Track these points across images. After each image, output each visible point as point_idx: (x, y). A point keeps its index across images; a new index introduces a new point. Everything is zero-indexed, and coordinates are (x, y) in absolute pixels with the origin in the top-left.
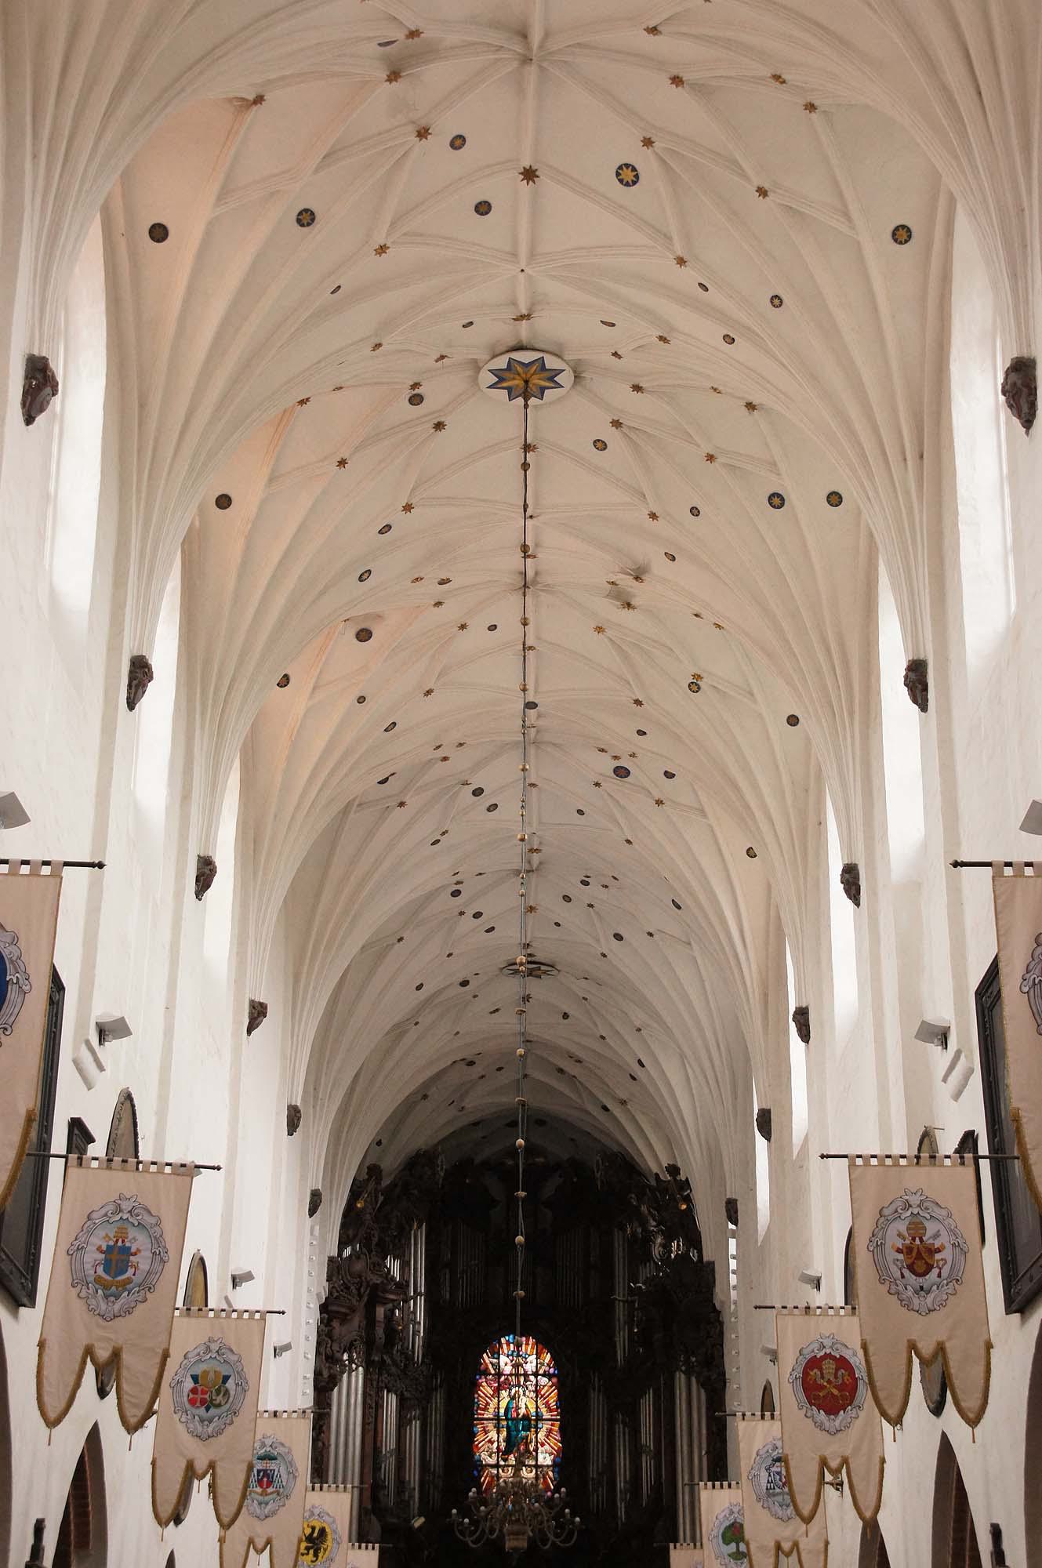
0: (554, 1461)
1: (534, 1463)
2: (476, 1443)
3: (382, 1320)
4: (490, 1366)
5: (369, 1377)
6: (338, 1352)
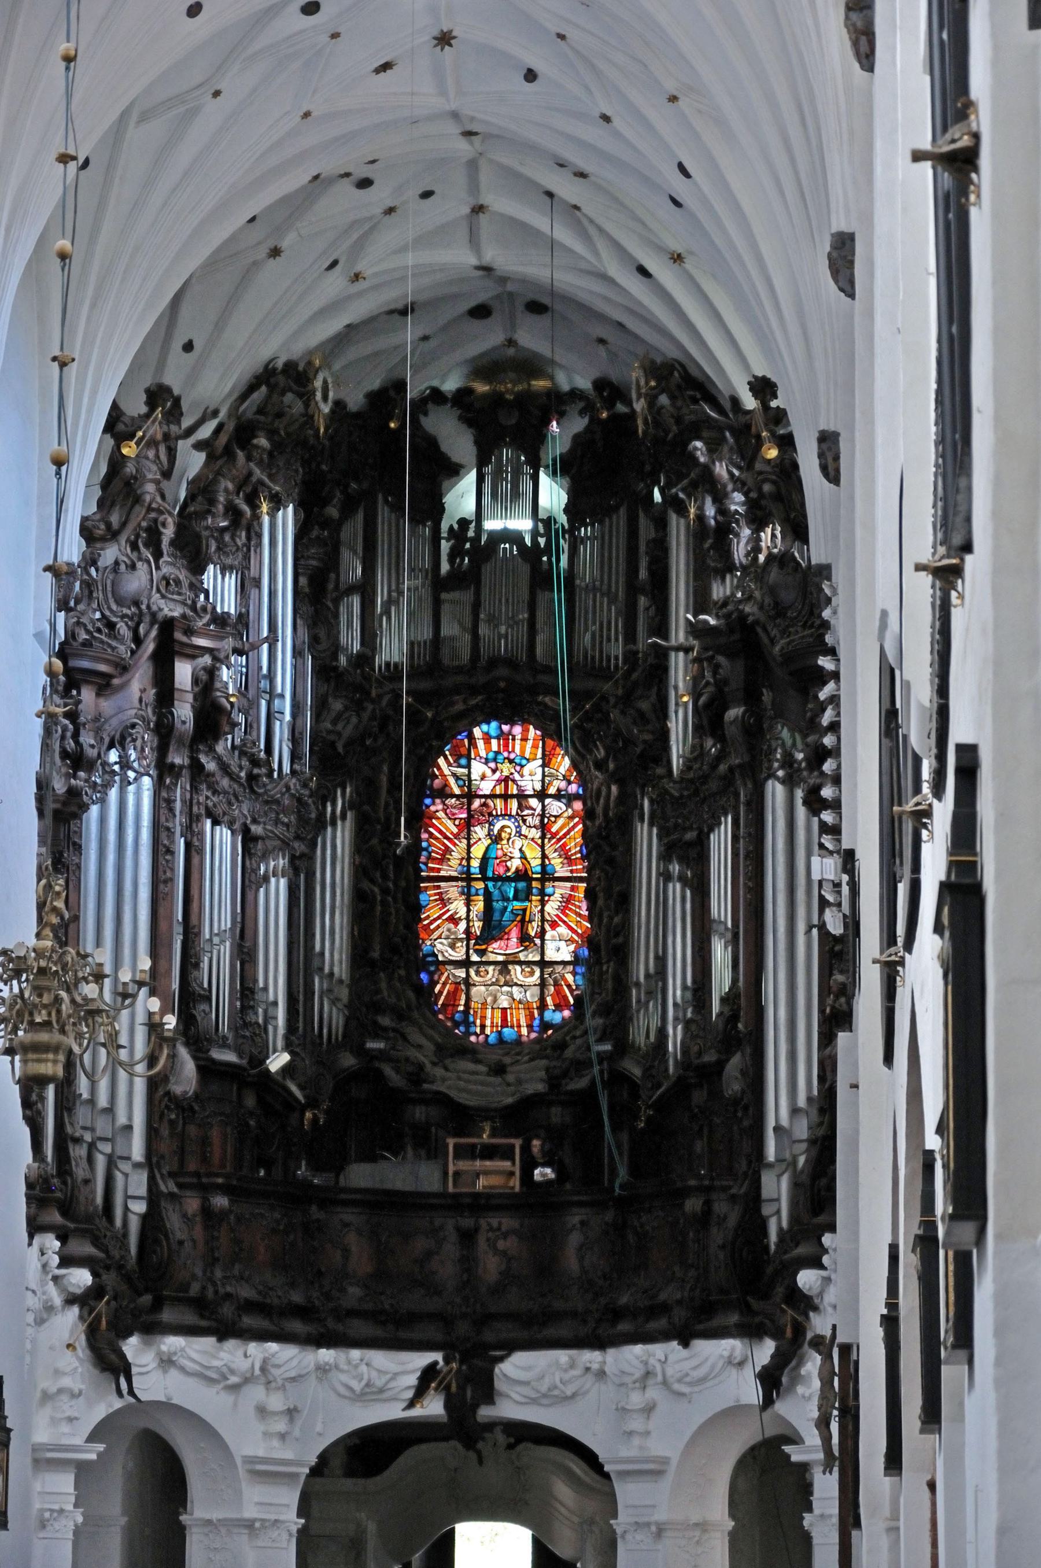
0: (575, 953)
1: (537, 958)
2: (426, 922)
3: (189, 688)
4: (452, 781)
5: (164, 794)
6: (93, 746)
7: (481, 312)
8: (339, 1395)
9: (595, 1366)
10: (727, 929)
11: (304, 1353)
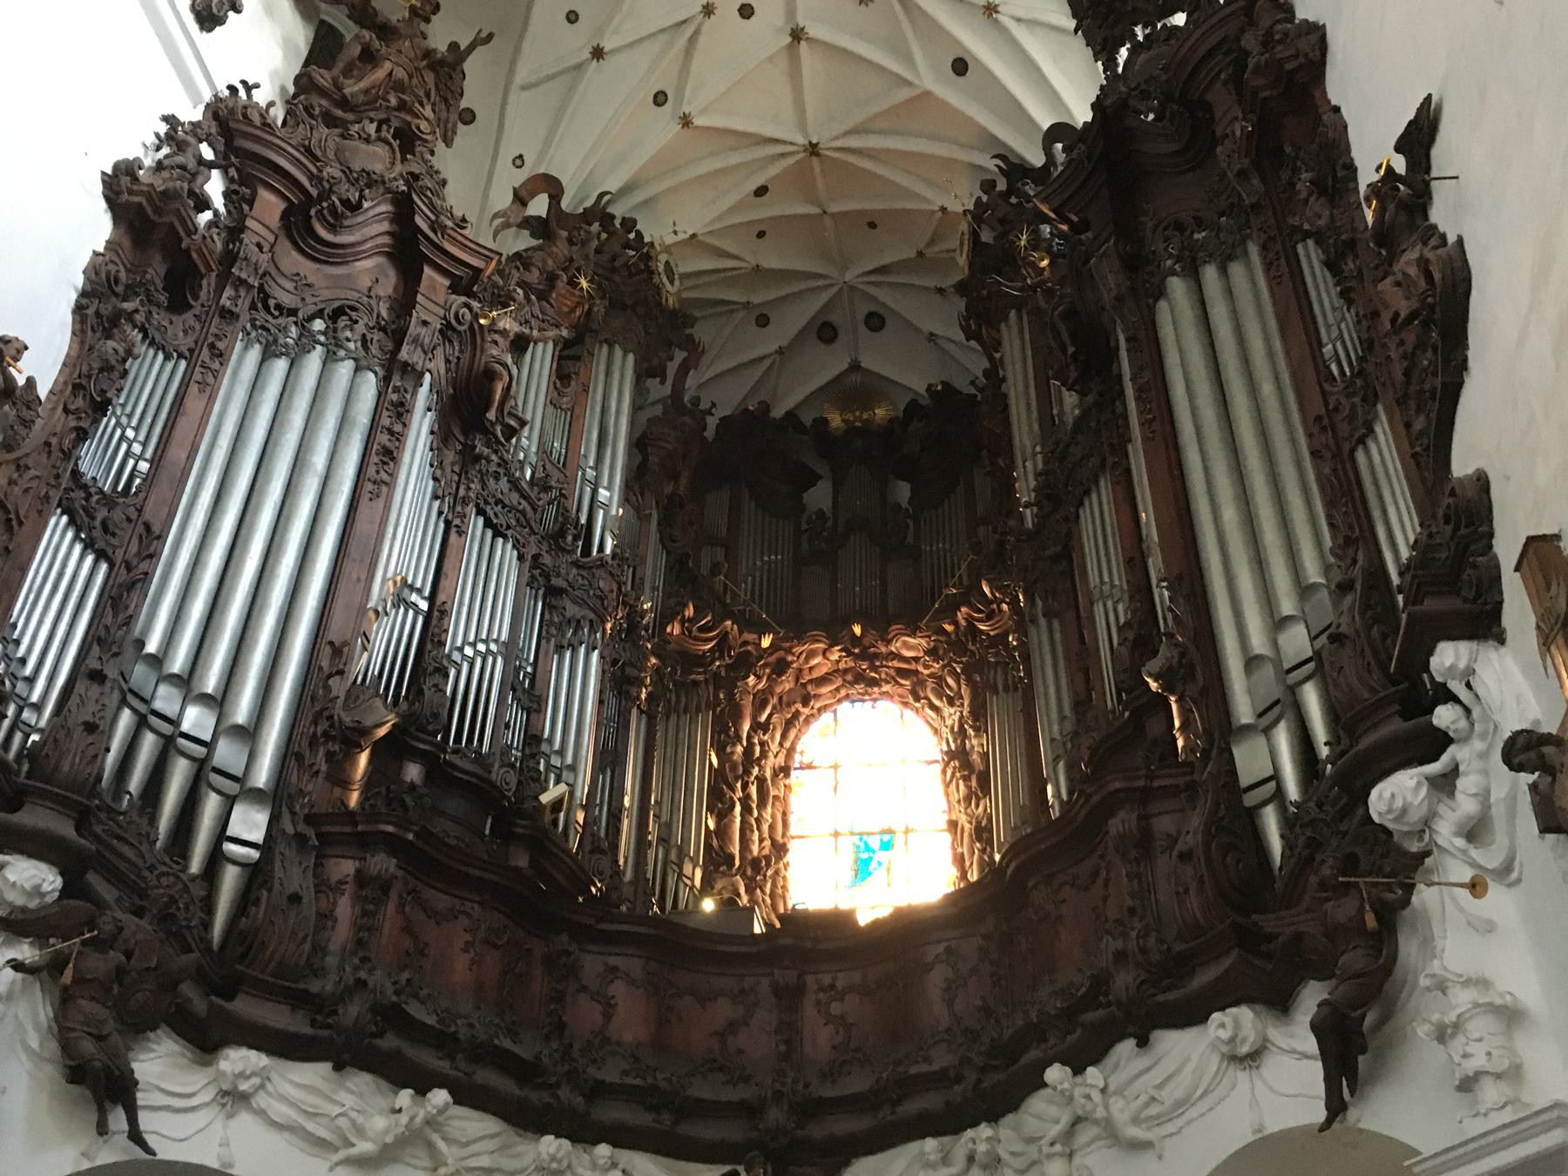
7: (826, 332)
9: (982, 1148)
10: (1113, 586)
11: (517, 1139)
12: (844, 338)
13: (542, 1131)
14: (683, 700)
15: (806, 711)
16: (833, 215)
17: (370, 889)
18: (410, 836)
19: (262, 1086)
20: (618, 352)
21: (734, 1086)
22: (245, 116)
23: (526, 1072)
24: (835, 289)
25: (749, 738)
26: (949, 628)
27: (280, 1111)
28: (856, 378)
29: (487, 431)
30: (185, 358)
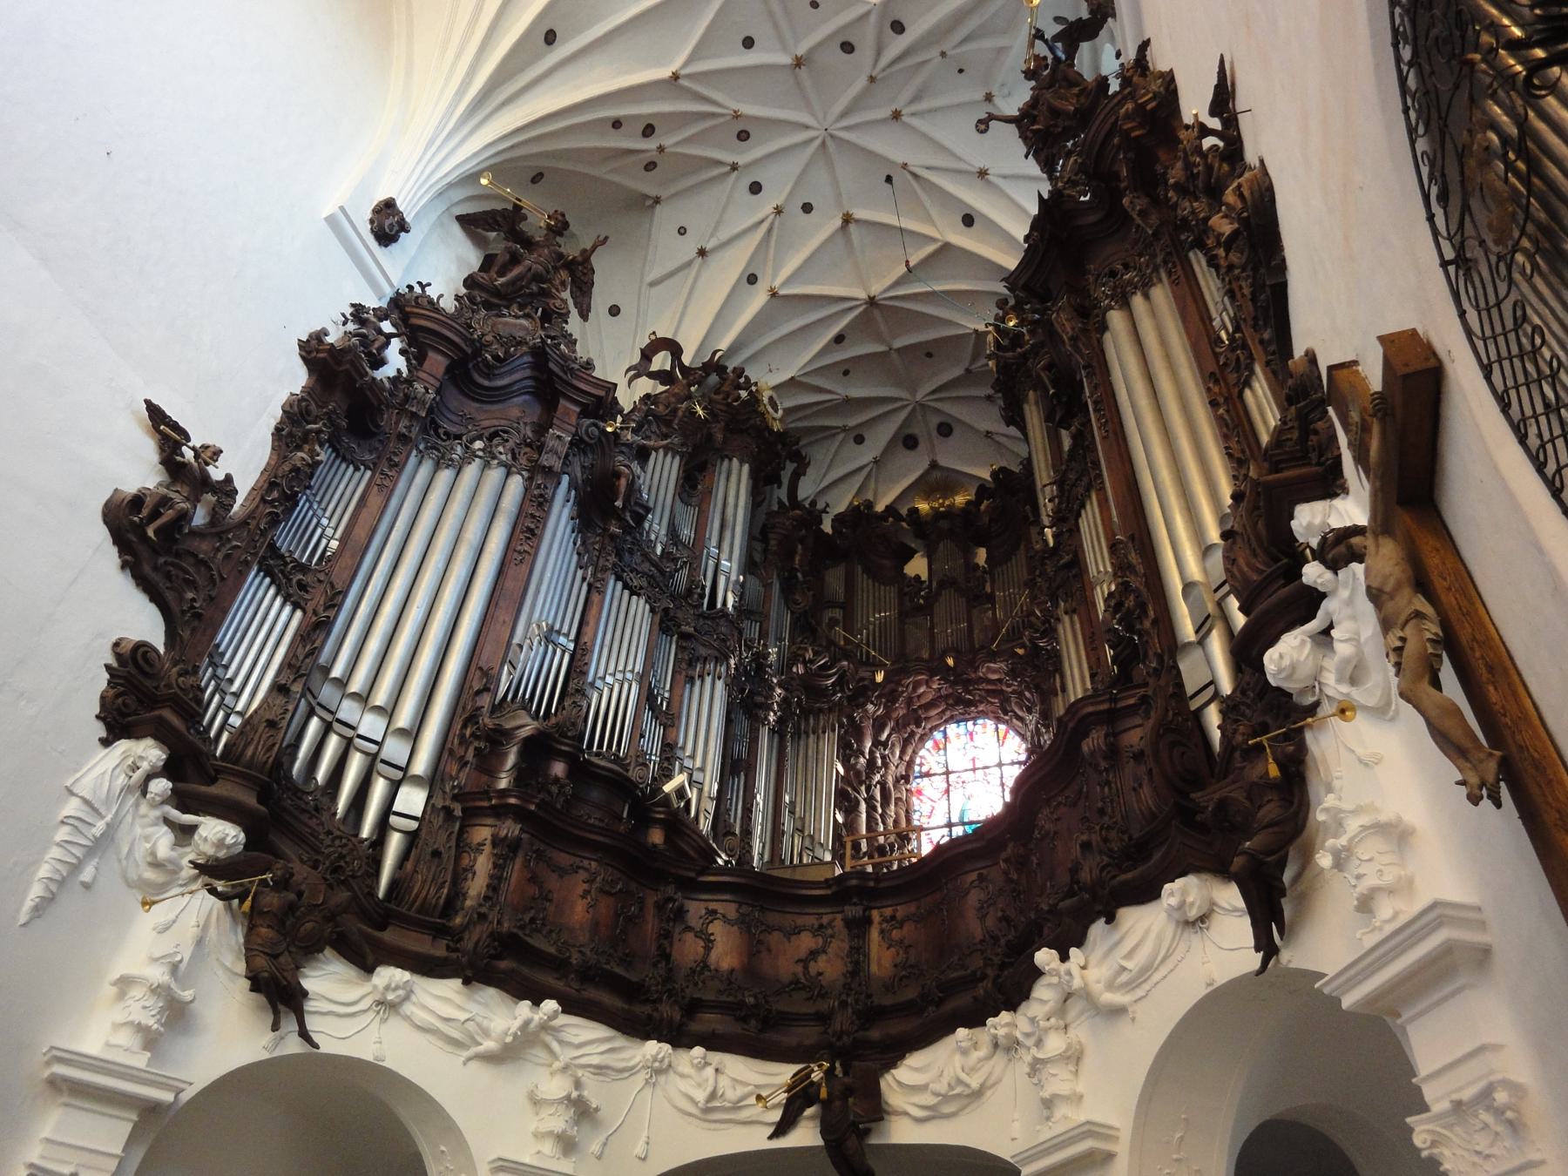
7: (910, 442)
8: (675, 1107)
12: (922, 447)
13: (646, 1037)
14: (812, 721)
15: (920, 731)
16: (898, 350)
17: (506, 850)
18: (533, 807)
19: (407, 998)
20: (735, 461)
21: (815, 1001)
22: (417, 303)
23: (632, 991)
24: (910, 408)
25: (871, 752)
26: (1020, 651)
27: (421, 1016)
28: (937, 474)
29: (621, 519)
30: (370, 469)
